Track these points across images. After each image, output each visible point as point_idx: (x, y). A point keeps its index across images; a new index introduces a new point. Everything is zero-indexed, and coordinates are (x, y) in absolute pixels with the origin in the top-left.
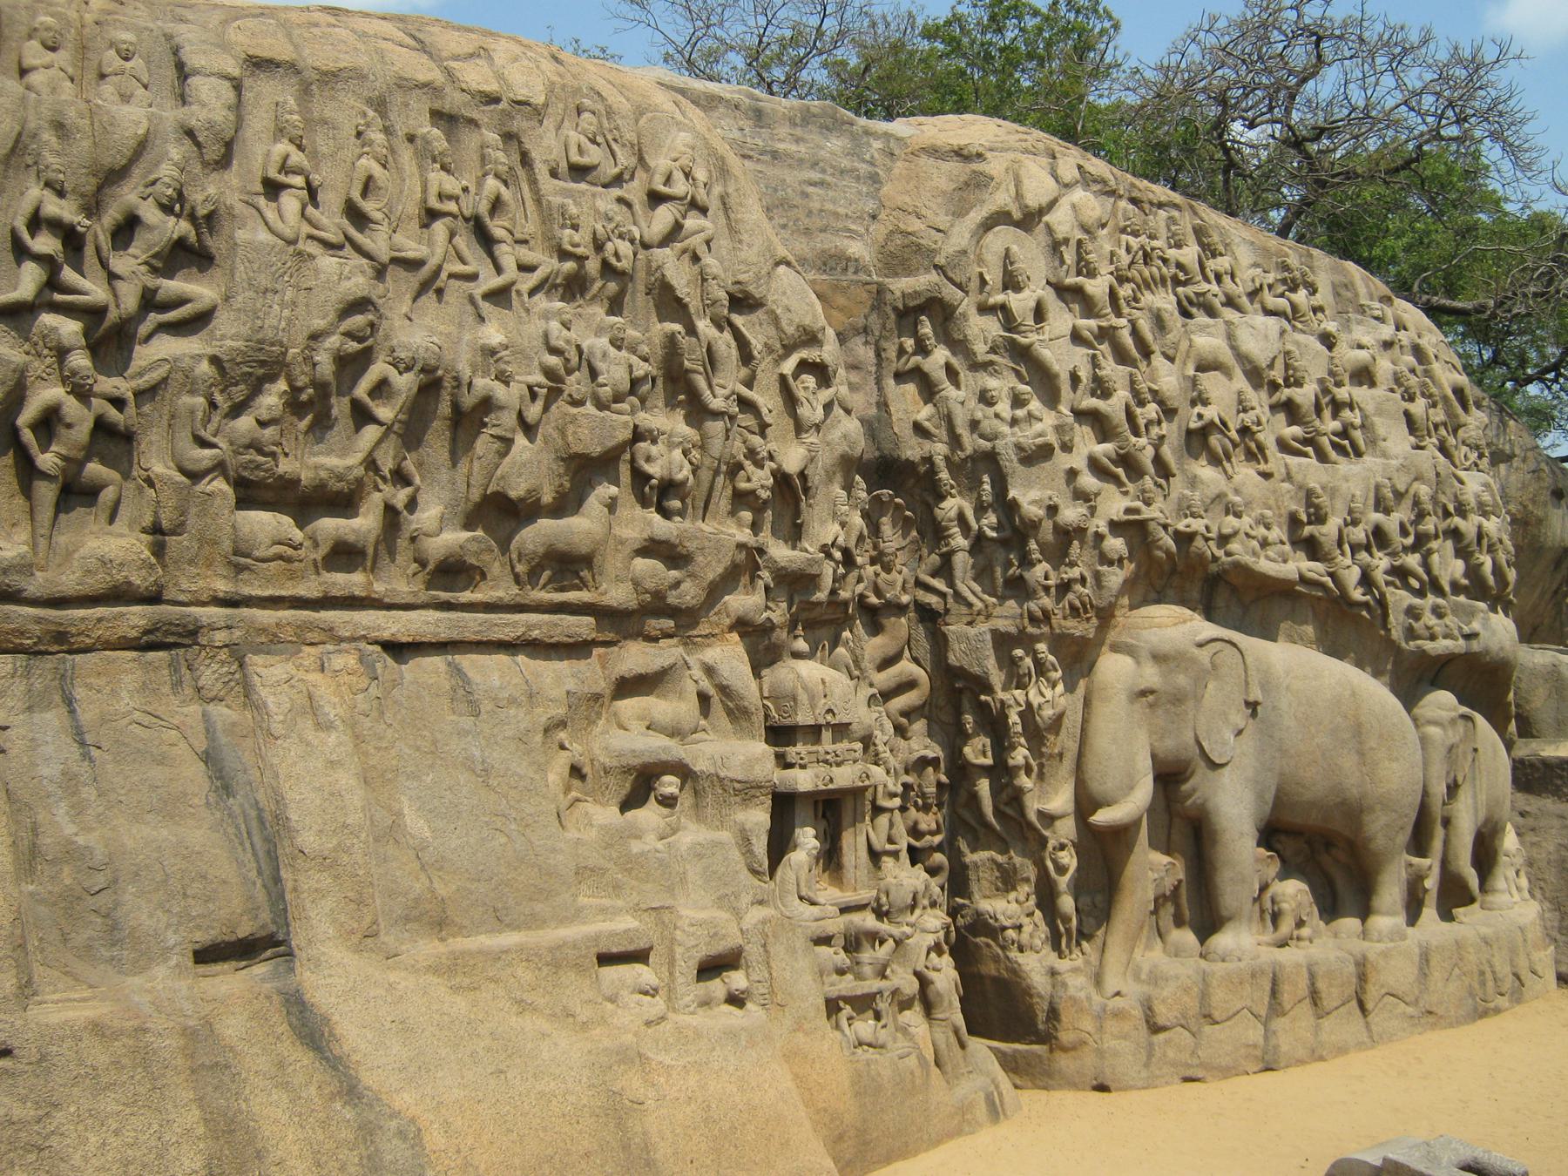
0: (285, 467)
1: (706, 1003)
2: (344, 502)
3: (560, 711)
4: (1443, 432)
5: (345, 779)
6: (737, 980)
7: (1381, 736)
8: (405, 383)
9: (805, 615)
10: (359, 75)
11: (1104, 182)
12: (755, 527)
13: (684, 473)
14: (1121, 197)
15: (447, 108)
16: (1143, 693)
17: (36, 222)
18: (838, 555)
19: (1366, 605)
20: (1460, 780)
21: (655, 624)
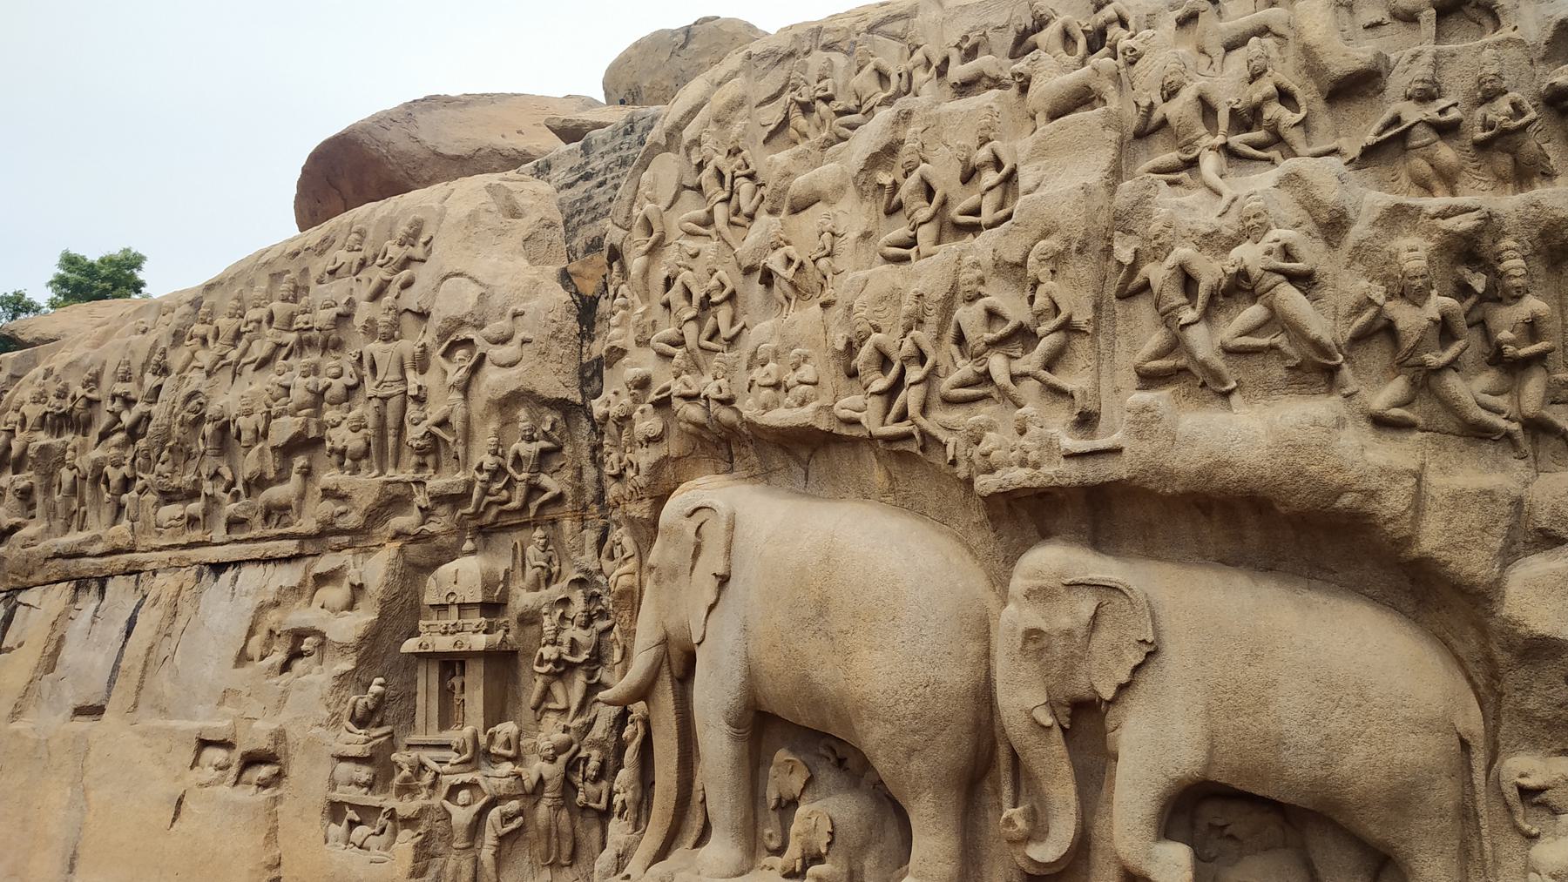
0: (176, 482)
1: (249, 783)
2: (193, 495)
3: (270, 598)
4: (1274, 110)
5: (152, 632)
6: (265, 771)
7: (855, 615)
8: (208, 428)
9: (472, 524)
10: (242, 272)
11: (774, 53)
12: (421, 466)
13: (355, 442)
14: (807, 53)
15: (277, 269)
16: (651, 568)
17: (114, 398)
18: (485, 476)
19: (908, 436)
20: (1108, 693)
21: (335, 540)
